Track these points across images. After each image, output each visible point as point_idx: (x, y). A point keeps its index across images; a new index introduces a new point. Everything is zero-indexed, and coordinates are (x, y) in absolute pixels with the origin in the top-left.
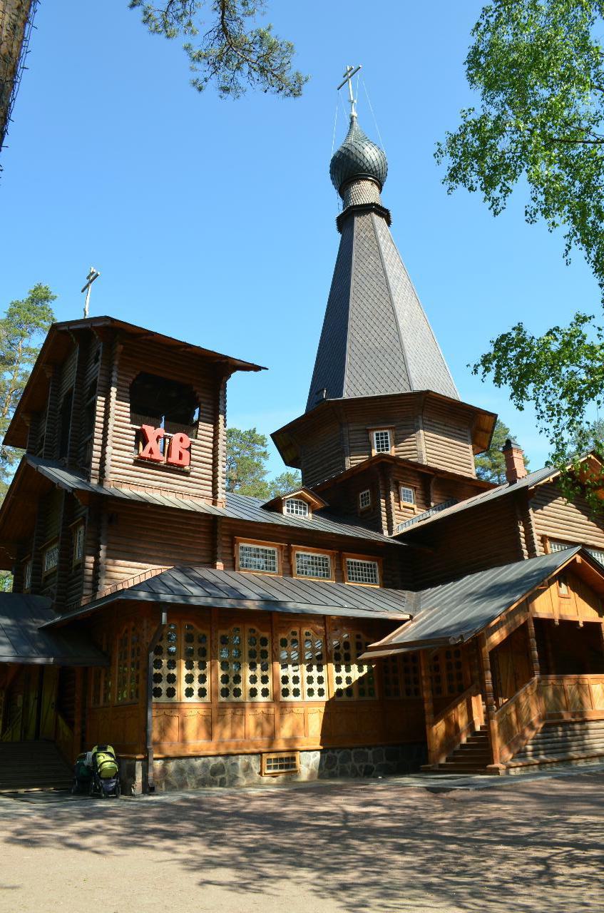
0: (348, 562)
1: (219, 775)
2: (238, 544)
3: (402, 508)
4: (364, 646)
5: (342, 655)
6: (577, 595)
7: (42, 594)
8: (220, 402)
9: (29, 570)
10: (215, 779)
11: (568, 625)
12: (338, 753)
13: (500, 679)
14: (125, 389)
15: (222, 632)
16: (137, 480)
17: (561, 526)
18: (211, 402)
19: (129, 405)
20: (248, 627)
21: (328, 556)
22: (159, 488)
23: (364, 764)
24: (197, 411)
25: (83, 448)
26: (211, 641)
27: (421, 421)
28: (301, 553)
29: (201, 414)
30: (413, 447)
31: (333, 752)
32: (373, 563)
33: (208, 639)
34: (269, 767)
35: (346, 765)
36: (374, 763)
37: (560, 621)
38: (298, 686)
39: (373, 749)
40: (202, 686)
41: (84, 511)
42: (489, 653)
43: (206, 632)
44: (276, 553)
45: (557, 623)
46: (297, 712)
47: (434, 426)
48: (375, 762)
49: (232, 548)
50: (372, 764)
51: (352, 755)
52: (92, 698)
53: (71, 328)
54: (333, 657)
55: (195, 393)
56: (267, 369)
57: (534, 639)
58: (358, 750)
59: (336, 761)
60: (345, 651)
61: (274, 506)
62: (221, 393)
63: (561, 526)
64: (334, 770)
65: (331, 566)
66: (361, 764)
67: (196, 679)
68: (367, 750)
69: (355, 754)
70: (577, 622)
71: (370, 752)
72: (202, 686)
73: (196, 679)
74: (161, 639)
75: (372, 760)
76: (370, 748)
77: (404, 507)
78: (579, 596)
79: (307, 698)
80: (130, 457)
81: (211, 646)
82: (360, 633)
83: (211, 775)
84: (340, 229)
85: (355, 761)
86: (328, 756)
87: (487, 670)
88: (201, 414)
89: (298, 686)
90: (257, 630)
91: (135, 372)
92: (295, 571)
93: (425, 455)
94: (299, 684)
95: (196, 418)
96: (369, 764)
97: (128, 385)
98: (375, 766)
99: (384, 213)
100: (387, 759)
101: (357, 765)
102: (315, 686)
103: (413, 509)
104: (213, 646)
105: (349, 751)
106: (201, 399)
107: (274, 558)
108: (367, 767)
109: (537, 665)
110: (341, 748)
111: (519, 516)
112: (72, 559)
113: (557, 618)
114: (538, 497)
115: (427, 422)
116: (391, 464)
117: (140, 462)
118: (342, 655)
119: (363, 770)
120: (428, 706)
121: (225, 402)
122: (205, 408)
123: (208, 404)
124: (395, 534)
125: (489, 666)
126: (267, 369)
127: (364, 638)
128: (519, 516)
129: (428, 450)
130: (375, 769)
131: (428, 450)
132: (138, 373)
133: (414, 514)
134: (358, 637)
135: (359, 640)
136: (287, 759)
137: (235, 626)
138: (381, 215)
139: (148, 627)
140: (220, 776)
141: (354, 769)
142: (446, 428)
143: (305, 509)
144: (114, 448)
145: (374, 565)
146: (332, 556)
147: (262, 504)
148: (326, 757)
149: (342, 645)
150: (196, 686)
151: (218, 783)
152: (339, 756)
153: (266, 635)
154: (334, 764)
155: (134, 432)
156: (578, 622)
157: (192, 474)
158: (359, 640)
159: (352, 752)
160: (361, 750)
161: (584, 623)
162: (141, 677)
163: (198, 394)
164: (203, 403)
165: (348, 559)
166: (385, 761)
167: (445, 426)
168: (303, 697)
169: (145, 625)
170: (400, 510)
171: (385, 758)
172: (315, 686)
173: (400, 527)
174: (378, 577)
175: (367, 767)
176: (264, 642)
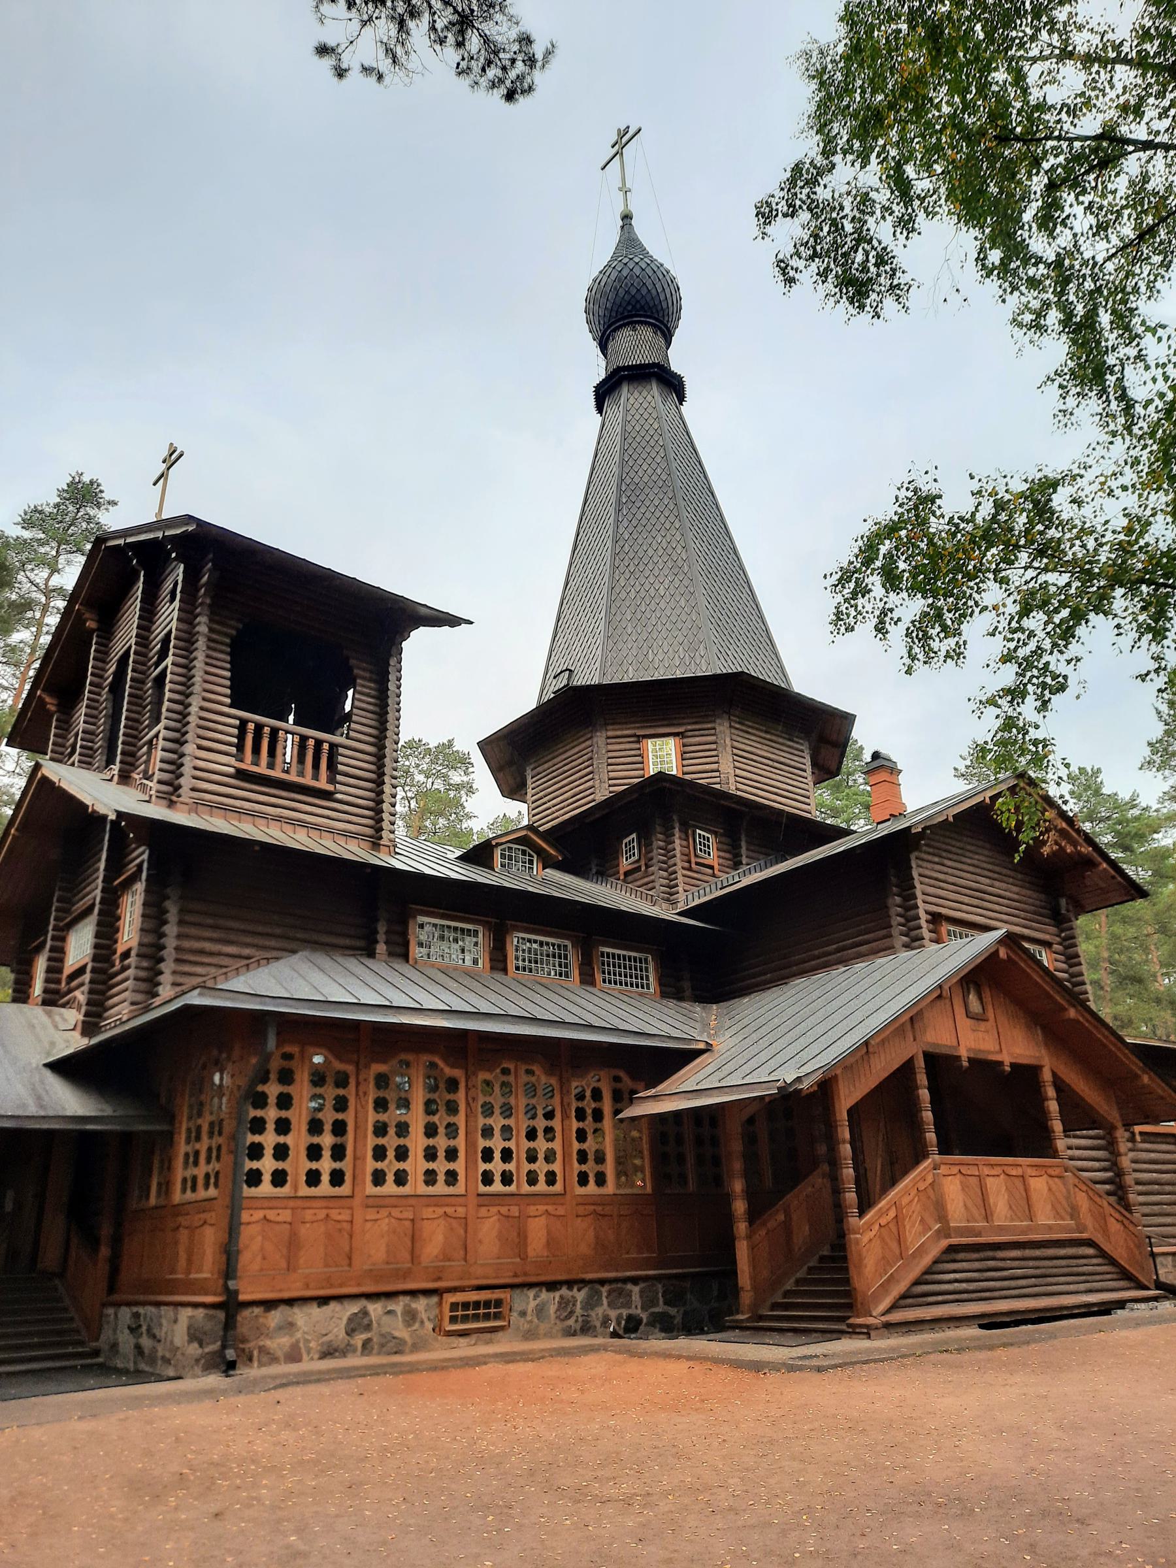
0: (602, 954)
1: (362, 1333)
2: (415, 917)
3: (693, 866)
4: (626, 1096)
5: (589, 1111)
7: (63, 1006)
8: (390, 677)
9: (41, 965)
10: (352, 1342)
11: (983, 1066)
12: (579, 1290)
13: (864, 1162)
14: (224, 648)
15: (378, 1068)
16: (238, 803)
17: (966, 899)
18: (374, 677)
19: (228, 674)
20: (426, 1058)
21: (567, 943)
22: (278, 819)
23: (625, 1312)
24: (350, 693)
25: (145, 749)
26: (358, 1084)
27: (727, 724)
30: (714, 766)
31: (570, 1288)
33: (352, 1081)
34: (453, 1320)
35: (593, 1314)
37: (970, 1060)
38: (511, 1166)
39: (642, 1285)
40: (337, 1165)
41: (141, 855)
42: (849, 1111)
43: (350, 1068)
44: (480, 935)
45: (965, 1064)
48: (644, 1308)
49: (405, 924)
50: (639, 1311)
51: (605, 1294)
52: (136, 1193)
53: (129, 540)
54: (573, 1114)
55: (348, 658)
56: (472, 623)
57: (926, 1091)
58: (614, 1286)
59: (574, 1305)
60: (593, 1105)
61: (480, 855)
62: (393, 661)
63: (966, 899)
64: (571, 1322)
65: (573, 958)
66: (619, 1311)
67: (326, 1154)
68: (629, 1286)
69: (610, 1293)
70: (1000, 1063)
71: (636, 1290)
72: (337, 1165)
73: (326, 1154)
74: (265, 1080)
76: (635, 1280)
77: (697, 864)
79: (526, 1189)
80: (227, 764)
81: (357, 1095)
82: (622, 1074)
83: (347, 1334)
84: (600, 408)
85: (609, 1305)
86: (561, 1297)
87: (844, 1142)
88: (357, 703)
89: (511, 1166)
90: (441, 1064)
92: (511, 964)
93: (732, 780)
94: (514, 1163)
95: (348, 708)
96: (632, 1311)
98: (644, 1316)
100: (665, 1303)
101: (613, 1314)
102: (541, 1167)
103: (712, 867)
104: (361, 1093)
105: (598, 1286)
106: (356, 671)
108: (630, 1318)
109: (931, 1136)
110: (583, 1283)
111: (894, 880)
112: (116, 942)
113: (964, 1053)
114: (924, 848)
115: (737, 726)
117: (241, 775)
118: (589, 1111)
119: (623, 1322)
120: (740, 1207)
121: (399, 679)
122: (363, 686)
123: (370, 680)
124: (681, 907)
125: (847, 1136)
126: (472, 623)
127: (627, 1082)
128: (894, 880)
129: (738, 772)
130: (645, 1321)
131: (738, 772)
133: (714, 875)
134: (617, 1079)
135: (619, 1085)
136: (487, 1304)
137: (403, 1056)
139: (242, 1058)
140: (364, 1336)
141: (605, 1322)
142: (768, 736)
144: (200, 747)
145: (646, 960)
147: (458, 853)
148: (557, 1299)
149: (588, 1093)
150: (326, 1165)
151: (359, 1352)
152: (580, 1295)
153: (458, 1073)
154: (572, 1313)
155: (238, 722)
156: (1001, 1063)
157: (339, 796)
158: (619, 1085)
159: (604, 1290)
160: (619, 1285)
161: (1012, 1065)
162: (224, 1149)
164: (364, 678)
166: (660, 1308)
167: (766, 732)
168: (518, 1186)
169: (236, 1053)
170: (690, 869)
172: (541, 1167)
173: (690, 897)
174: (651, 979)
175: (630, 1318)
176: (453, 1085)
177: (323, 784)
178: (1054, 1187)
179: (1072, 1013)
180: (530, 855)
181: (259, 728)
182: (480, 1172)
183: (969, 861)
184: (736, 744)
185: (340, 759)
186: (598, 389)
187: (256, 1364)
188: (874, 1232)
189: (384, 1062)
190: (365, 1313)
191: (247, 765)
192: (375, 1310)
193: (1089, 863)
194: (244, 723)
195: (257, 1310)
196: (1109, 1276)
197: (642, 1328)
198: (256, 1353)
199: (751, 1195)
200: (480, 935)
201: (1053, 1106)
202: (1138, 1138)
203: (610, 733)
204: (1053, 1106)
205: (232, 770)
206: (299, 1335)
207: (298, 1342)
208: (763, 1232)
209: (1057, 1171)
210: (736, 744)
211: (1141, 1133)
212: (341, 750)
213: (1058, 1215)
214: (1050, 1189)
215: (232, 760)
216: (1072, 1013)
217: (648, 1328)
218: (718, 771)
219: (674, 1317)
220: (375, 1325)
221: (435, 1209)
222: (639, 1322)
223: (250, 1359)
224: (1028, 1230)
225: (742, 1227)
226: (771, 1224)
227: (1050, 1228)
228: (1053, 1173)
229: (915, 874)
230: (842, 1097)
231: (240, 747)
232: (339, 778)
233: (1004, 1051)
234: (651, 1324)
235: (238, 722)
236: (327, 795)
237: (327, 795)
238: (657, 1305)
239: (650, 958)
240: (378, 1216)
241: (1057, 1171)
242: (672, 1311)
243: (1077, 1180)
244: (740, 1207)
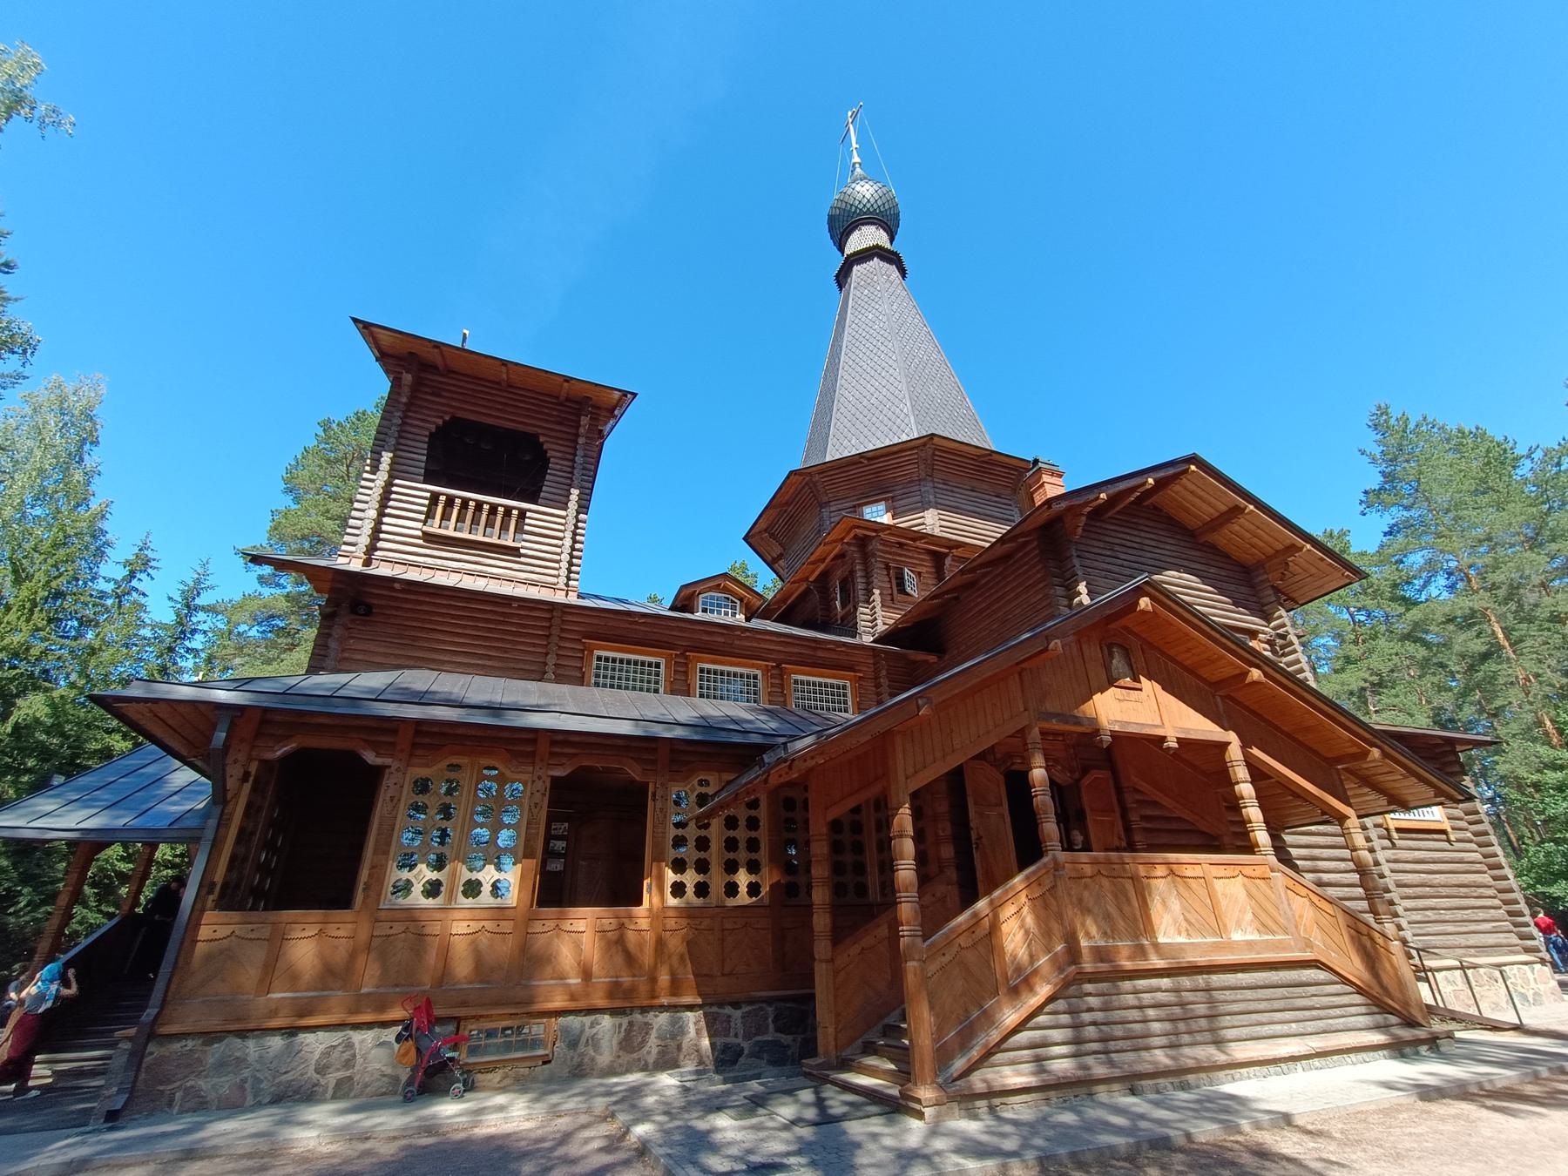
0: (796, 682)
2: (592, 651)
6: (1158, 687)
10: (323, 1082)
15: (423, 772)
28: (706, 666)
29: (590, 485)
32: (841, 682)
36: (747, 1037)
39: (746, 1009)
44: (662, 666)
46: (569, 928)
47: (952, 491)
48: (747, 1037)
50: (739, 1040)
55: (542, 444)
68: (728, 1010)
71: (737, 1014)
75: (740, 1036)
78: (1163, 689)
87: (901, 836)
91: (441, 417)
96: (731, 1040)
97: (428, 433)
98: (746, 1045)
99: (891, 258)
100: (778, 1030)
106: (550, 454)
107: (657, 674)
115: (941, 486)
116: (874, 537)
117: (429, 538)
120: (821, 921)
125: (910, 830)
130: (746, 1052)
132: (447, 418)
137: (454, 760)
138: (890, 261)
143: (734, 608)
146: (766, 670)
156: (1163, 739)
157: (522, 551)
161: (1179, 740)
163: (545, 447)
165: (794, 677)
171: (771, 1027)
174: (850, 703)
177: (510, 543)
178: (1254, 891)
179: (1256, 674)
180: (732, 602)
181: (465, 502)
182: (463, 881)
183: (1149, 555)
184: (940, 501)
185: (527, 521)
186: (837, 276)
187: (175, 1110)
188: (948, 958)
189: (427, 766)
190: (349, 1045)
191: (434, 528)
192: (363, 1041)
193: (1293, 549)
194: (434, 498)
195: (190, 1043)
196: (1353, 1010)
197: (742, 1060)
198: (178, 1095)
199: (836, 909)
200: (662, 666)
201: (1246, 789)
202: (1395, 835)
203: (833, 509)
204: (1246, 789)
205: (420, 533)
206: (246, 1073)
207: (244, 1081)
208: (854, 950)
209: (1259, 871)
210: (940, 501)
211: (1399, 830)
212: (528, 514)
213: (1264, 928)
214: (1250, 895)
215: (419, 525)
216: (1256, 674)
217: (750, 1061)
218: (923, 524)
219: (788, 1046)
220: (359, 1060)
221: (471, 923)
222: (739, 1053)
223: (170, 1104)
224: (1216, 947)
225: (822, 948)
226: (868, 940)
227: (1250, 945)
228: (1253, 874)
229: (1076, 562)
230: (902, 778)
231: (430, 515)
232: (525, 536)
233: (1167, 724)
234: (756, 1054)
235: (428, 495)
236: (514, 552)
237: (514, 552)
238: (766, 1032)
239: (848, 683)
240: (391, 932)
241: (1259, 871)
242: (786, 1039)
243: (1291, 883)
244: (821, 921)
